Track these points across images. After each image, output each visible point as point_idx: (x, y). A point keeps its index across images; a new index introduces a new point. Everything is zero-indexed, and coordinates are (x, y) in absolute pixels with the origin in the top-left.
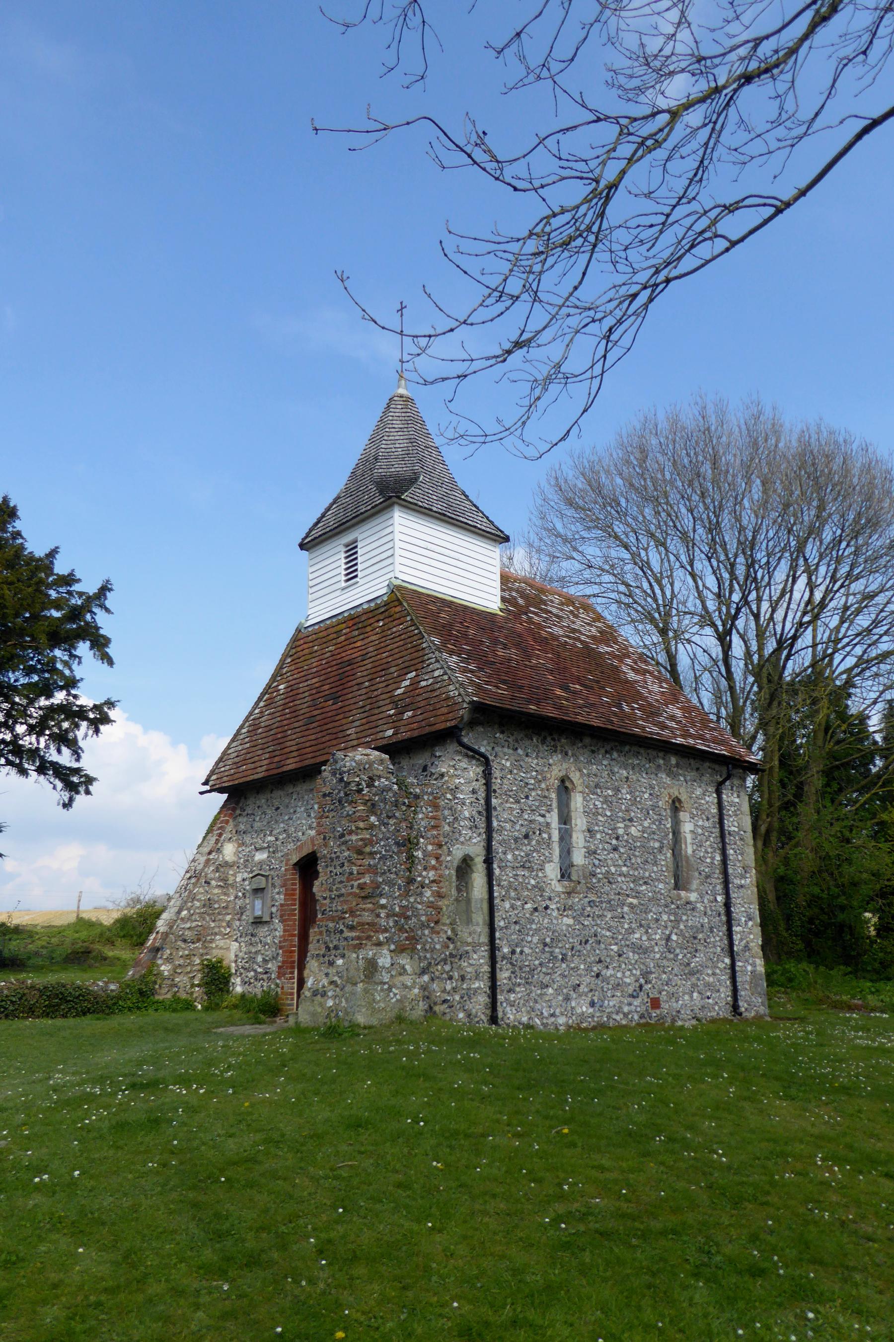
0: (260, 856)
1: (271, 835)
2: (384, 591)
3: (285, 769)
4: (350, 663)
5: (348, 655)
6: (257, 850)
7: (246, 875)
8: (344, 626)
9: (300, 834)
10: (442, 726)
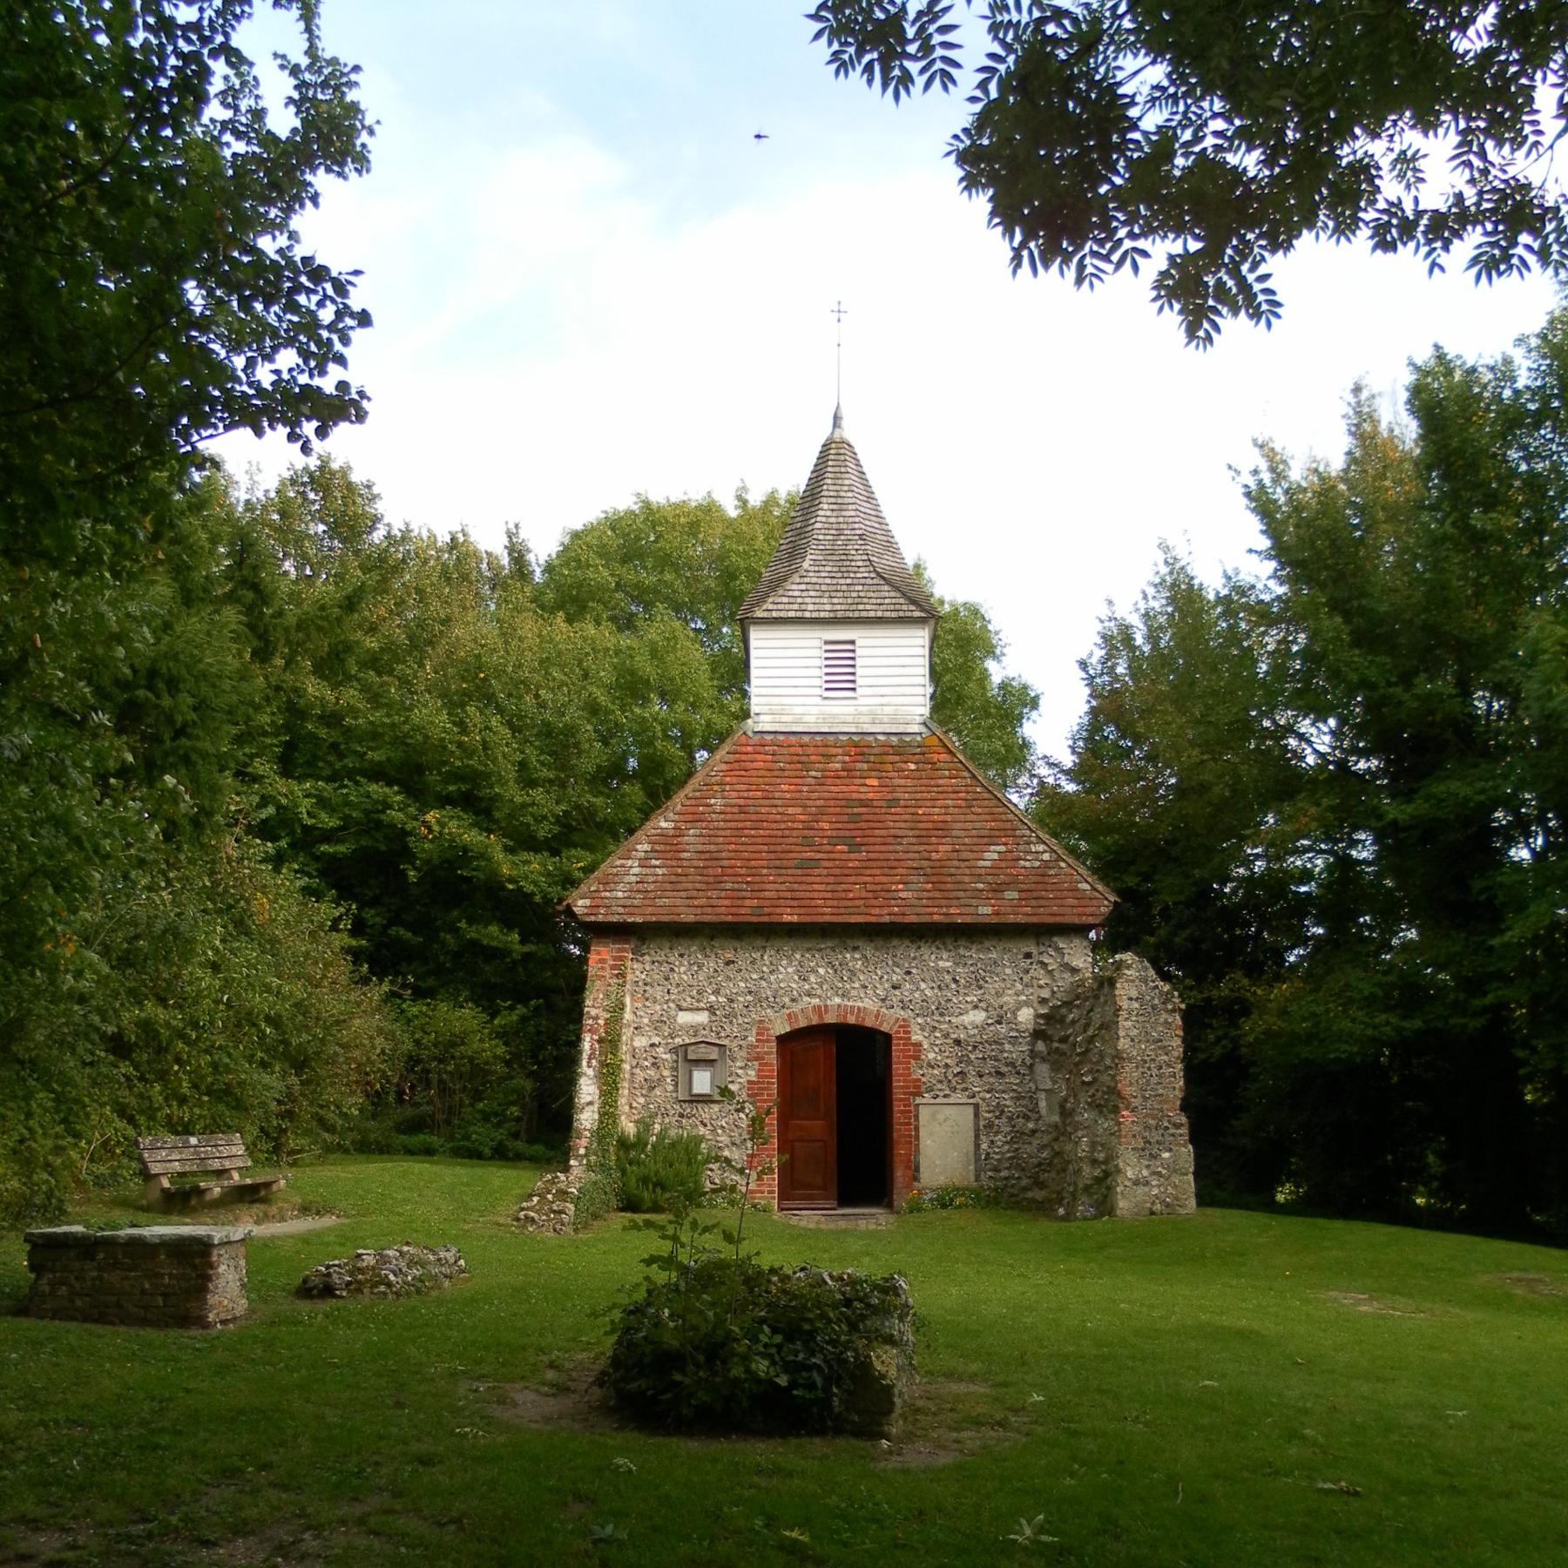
0: (684, 1018)
1: (716, 992)
2: (915, 728)
3: (775, 919)
4: (864, 803)
7: (656, 1040)
8: (840, 751)
9: (787, 1000)
10: (1076, 920)
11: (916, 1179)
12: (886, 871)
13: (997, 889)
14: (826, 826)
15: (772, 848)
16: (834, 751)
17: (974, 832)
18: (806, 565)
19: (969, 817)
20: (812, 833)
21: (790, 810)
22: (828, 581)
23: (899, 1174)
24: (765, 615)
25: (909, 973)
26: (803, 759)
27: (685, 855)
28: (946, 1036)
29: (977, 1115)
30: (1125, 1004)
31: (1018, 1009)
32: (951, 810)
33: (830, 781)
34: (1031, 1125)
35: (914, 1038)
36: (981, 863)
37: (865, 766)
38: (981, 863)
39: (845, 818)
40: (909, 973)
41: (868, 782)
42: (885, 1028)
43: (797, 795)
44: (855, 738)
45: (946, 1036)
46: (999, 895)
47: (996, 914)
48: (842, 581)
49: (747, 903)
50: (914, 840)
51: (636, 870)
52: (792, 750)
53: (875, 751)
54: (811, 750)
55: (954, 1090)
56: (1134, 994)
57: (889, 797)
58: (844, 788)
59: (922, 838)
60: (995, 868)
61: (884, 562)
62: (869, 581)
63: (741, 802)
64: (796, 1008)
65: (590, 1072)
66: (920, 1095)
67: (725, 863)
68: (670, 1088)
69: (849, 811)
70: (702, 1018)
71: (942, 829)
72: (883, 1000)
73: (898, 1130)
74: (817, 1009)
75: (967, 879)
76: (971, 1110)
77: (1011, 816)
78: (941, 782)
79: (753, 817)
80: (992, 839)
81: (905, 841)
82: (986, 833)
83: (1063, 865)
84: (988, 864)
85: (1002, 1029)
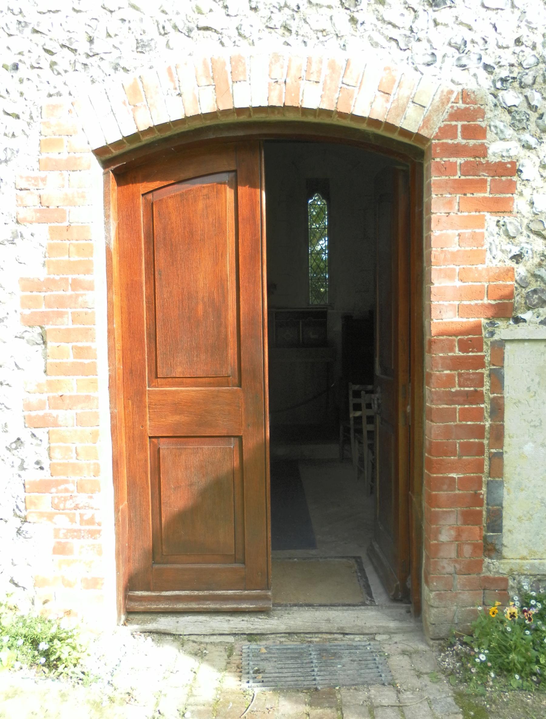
11: (491, 549)
23: (445, 534)
35: (496, 149)
42: (411, 121)
73: (441, 420)
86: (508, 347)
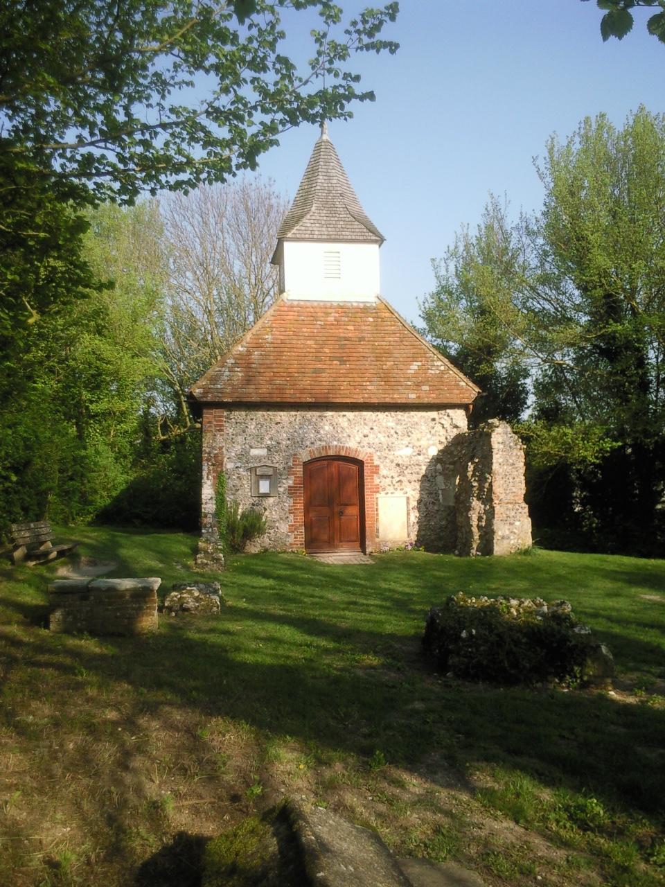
0: (254, 452)
4: (346, 339)
5: (341, 332)
6: (251, 447)
7: (239, 465)
8: (334, 311)
12: (360, 375)
13: (418, 385)
14: (327, 351)
15: (300, 362)
16: (330, 311)
17: (405, 355)
18: (313, 209)
19: (401, 347)
20: (320, 354)
21: (309, 342)
22: (325, 218)
24: (293, 236)
25: (372, 429)
26: (314, 315)
27: (253, 366)
28: (392, 462)
29: (408, 503)
30: (495, 445)
31: (429, 447)
32: (392, 343)
33: (328, 327)
34: (436, 508)
35: (376, 462)
36: (409, 371)
37: (346, 319)
38: (409, 371)
39: (337, 347)
40: (372, 429)
41: (349, 327)
42: (360, 458)
43: (312, 334)
44: (341, 304)
45: (392, 462)
46: (419, 388)
47: (419, 397)
48: (332, 219)
49: (288, 391)
50: (374, 359)
51: (227, 373)
52: (308, 310)
53: (353, 311)
54: (318, 310)
55: (396, 489)
56: (500, 440)
57: (359, 336)
58: (337, 331)
59: (378, 358)
60: (416, 374)
61: (353, 209)
62: (347, 219)
63: (282, 337)
64: (313, 448)
65: (209, 483)
66: (378, 492)
67: (275, 370)
68: (248, 490)
69: (339, 343)
70: (264, 452)
71: (388, 353)
72: (359, 443)
74: (325, 448)
75: (402, 380)
76: (405, 499)
77: (423, 347)
78: (386, 328)
79: (289, 346)
80: (414, 358)
81: (369, 359)
82: (411, 355)
83: (451, 372)
84: (413, 372)
85: (421, 458)
86: (379, 499)
